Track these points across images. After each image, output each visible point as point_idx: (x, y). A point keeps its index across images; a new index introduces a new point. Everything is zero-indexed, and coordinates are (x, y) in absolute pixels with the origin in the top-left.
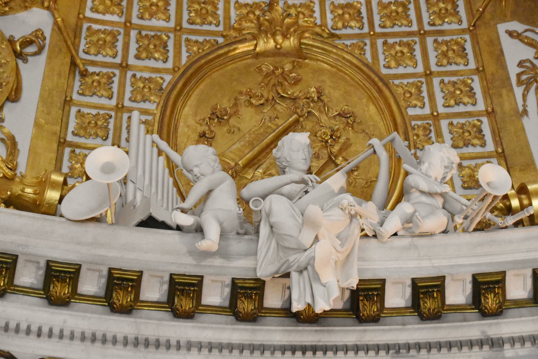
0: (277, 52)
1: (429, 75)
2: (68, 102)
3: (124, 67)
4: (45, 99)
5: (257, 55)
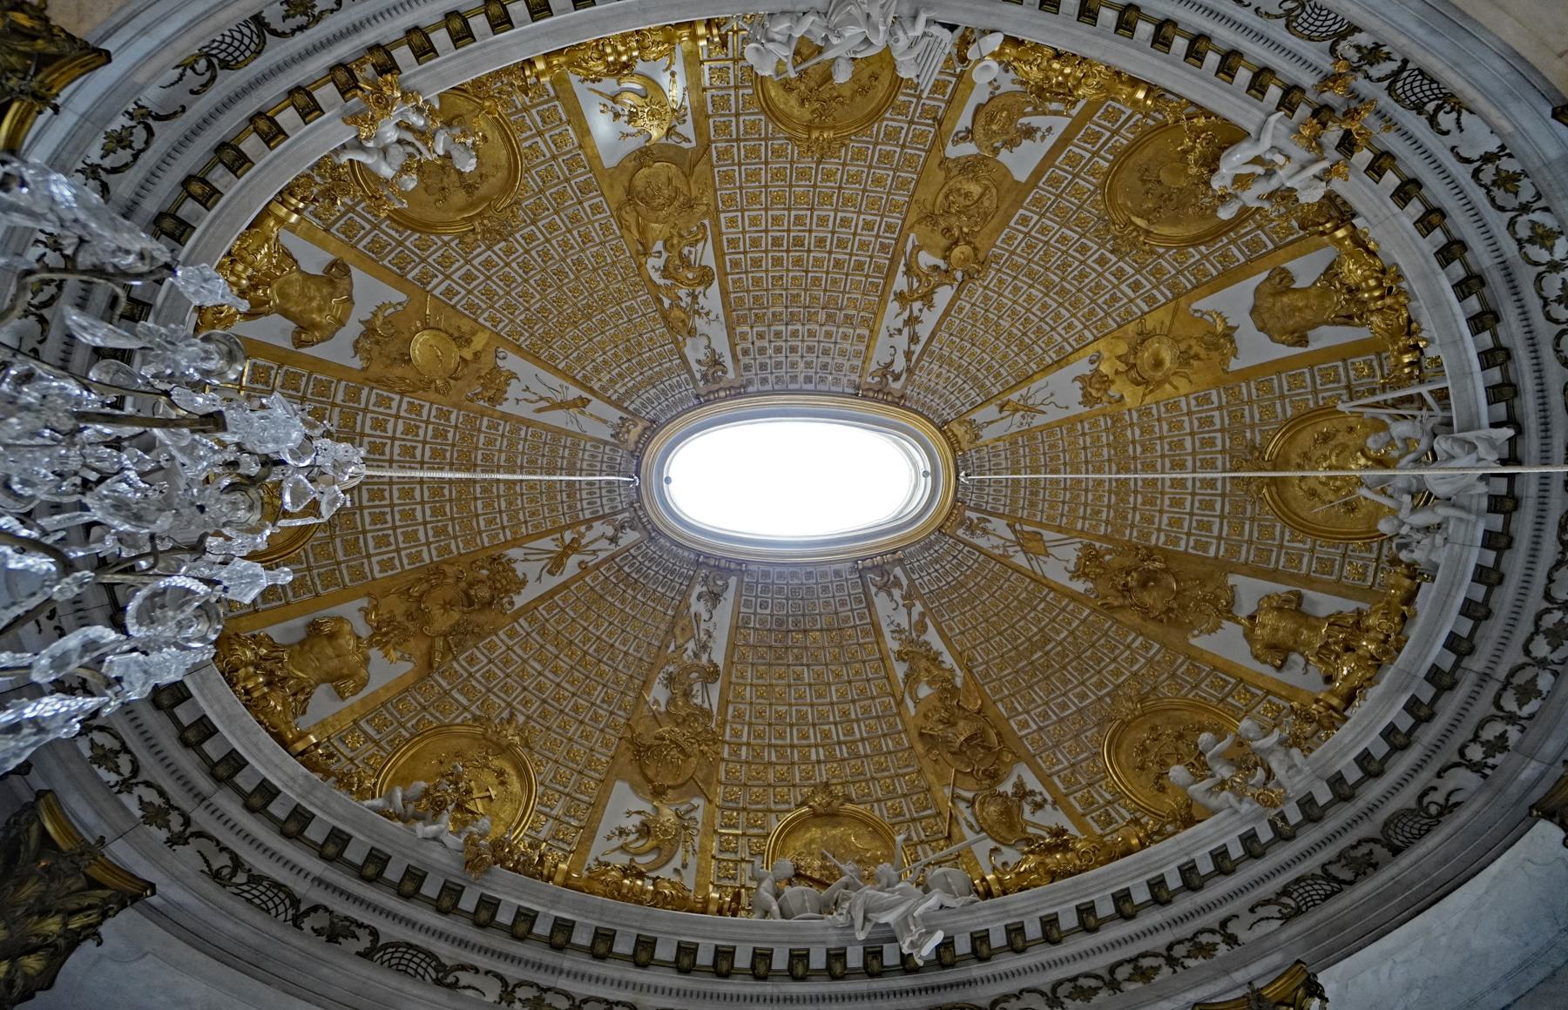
0: (822, 129)
1: (737, 115)
2: (950, 102)
3: (911, 122)
4: (963, 103)
5: (834, 127)
